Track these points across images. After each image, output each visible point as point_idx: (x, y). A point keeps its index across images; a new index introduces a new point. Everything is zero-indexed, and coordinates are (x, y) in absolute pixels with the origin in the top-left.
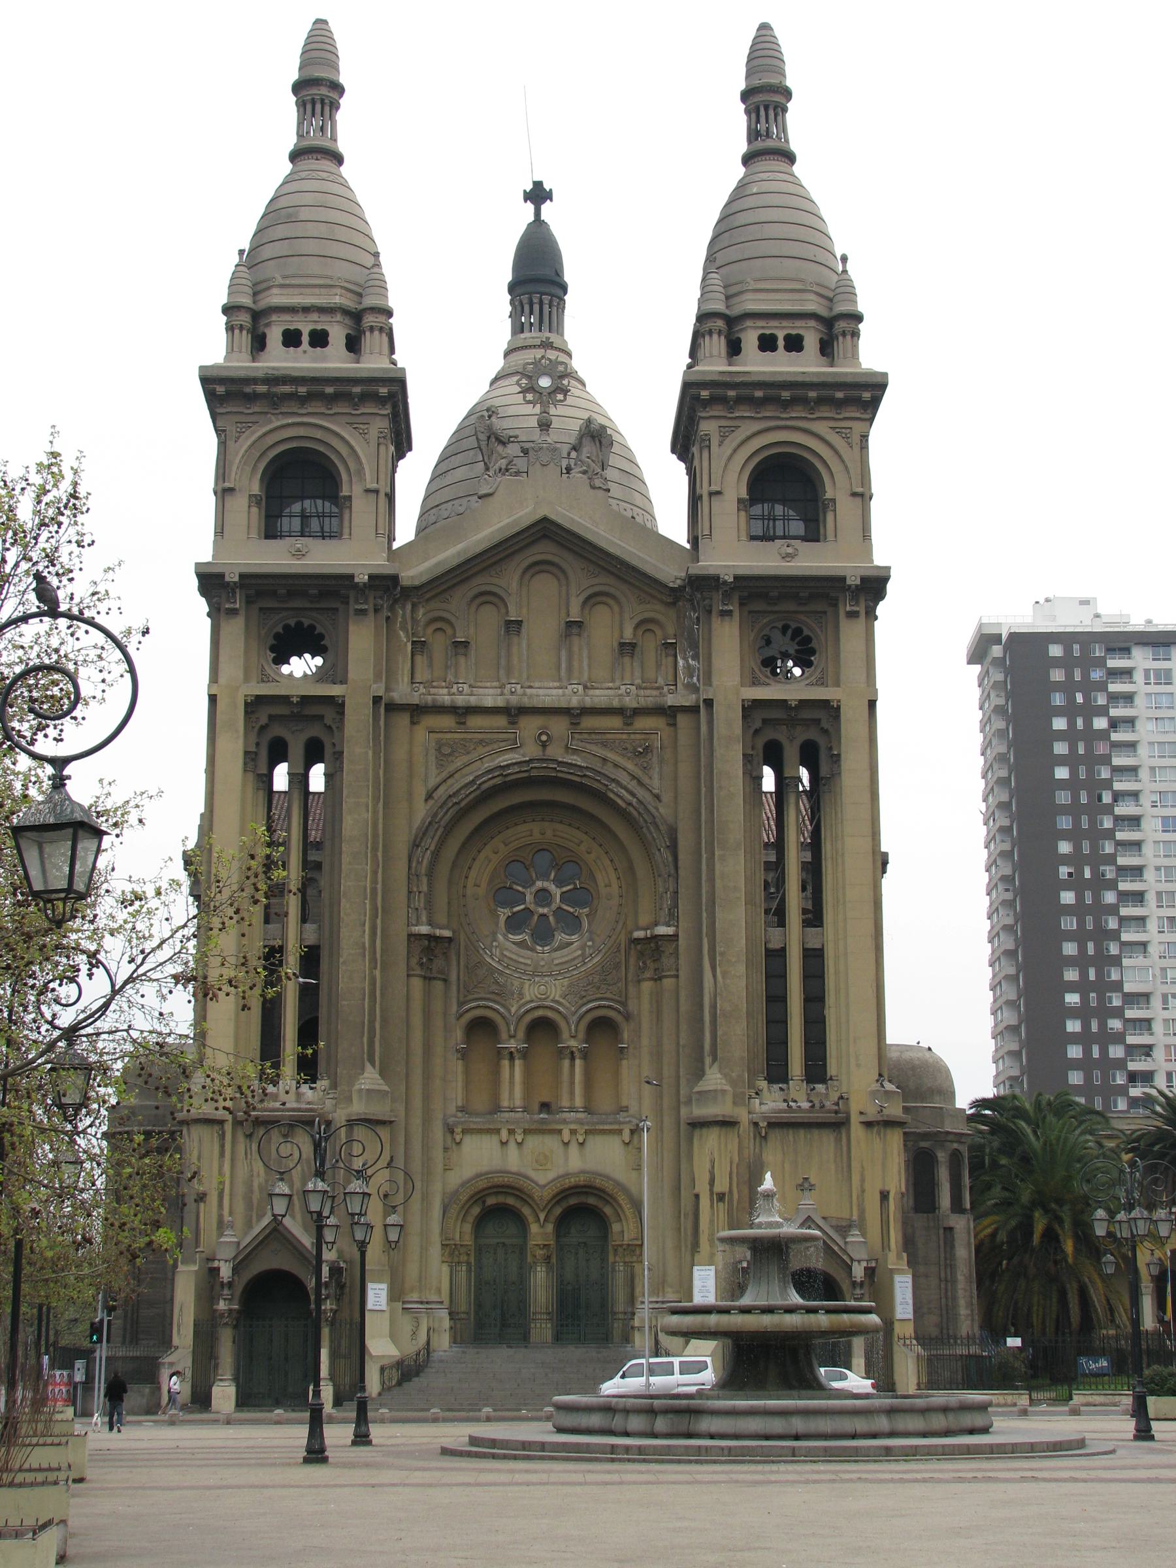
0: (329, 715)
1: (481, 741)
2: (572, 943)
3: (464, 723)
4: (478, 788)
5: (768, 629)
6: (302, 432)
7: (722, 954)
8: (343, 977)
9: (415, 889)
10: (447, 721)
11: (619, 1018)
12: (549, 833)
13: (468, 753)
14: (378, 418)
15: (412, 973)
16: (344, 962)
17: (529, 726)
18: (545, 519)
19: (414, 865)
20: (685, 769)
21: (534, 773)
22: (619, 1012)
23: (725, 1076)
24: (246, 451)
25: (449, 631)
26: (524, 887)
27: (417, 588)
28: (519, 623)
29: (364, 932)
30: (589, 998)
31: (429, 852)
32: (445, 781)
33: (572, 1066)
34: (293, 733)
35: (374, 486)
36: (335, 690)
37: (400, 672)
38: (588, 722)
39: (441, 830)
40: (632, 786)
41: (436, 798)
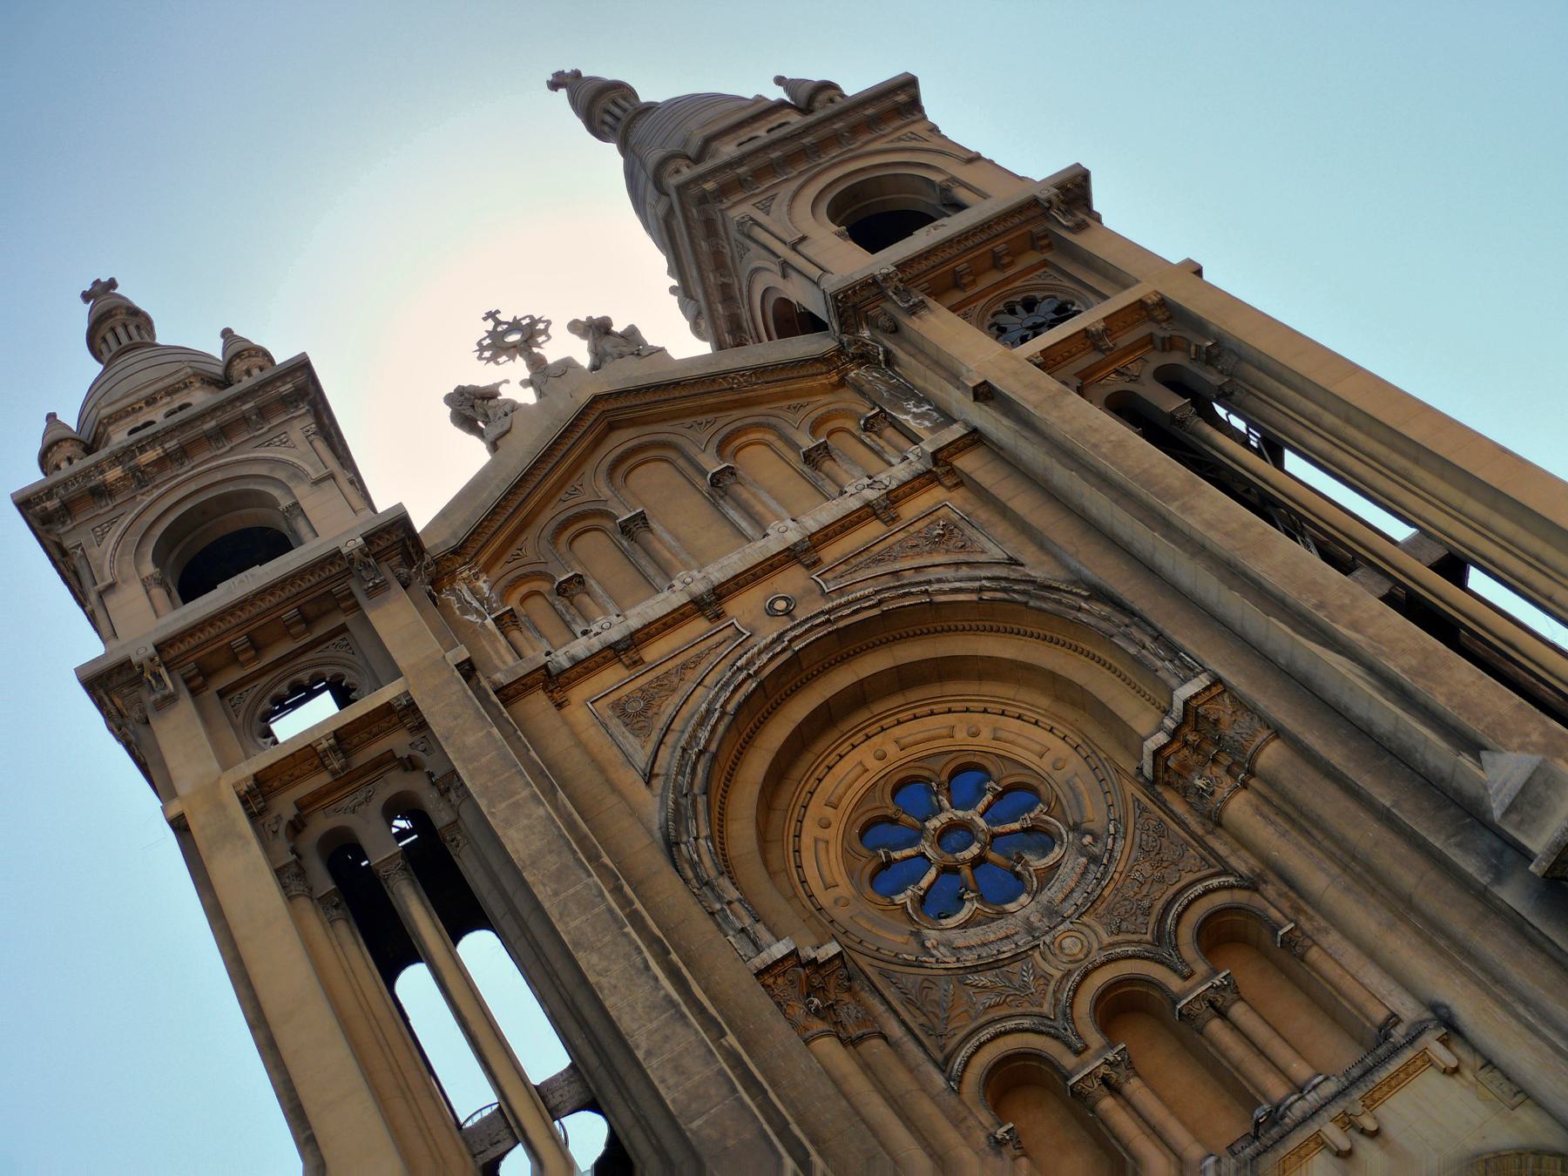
0: (399, 742)
1: (684, 666)
2: (1056, 866)
3: (640, 661)
4: (723, 713)
5: (989, 317)
6: (193, 487)
7: (1321, 606)
8: (663, 1081)
9: (718, 906)
10: (612, 676)
11: (1241, 897)
12: (892, 750)
13: (674, 690)
14: (295, 422)
15: (809, 1033)
16: (649, 1053)
17: (744, 608)
18: (596, 399)
19: (690, 874)
20: (1023, 502)
21: (797, 646)
22: (1231, 887)
23: (1522, 747)
24: (118, 543)
25: (544, 586)
26: (910, 843)
27: (457, 551)
28: (641, 517)
29: (656, 979)
30: (1159, 905)
31: (702, 841)
32: (661, 742)
33: (1235, 1027)
34: (354, 811)
35: (323, 472)
36: (389, 693)
37: (494, 656)
38: (832, 553)
39: (701, 800)
40: (965, 572)
41: (662, 771)
